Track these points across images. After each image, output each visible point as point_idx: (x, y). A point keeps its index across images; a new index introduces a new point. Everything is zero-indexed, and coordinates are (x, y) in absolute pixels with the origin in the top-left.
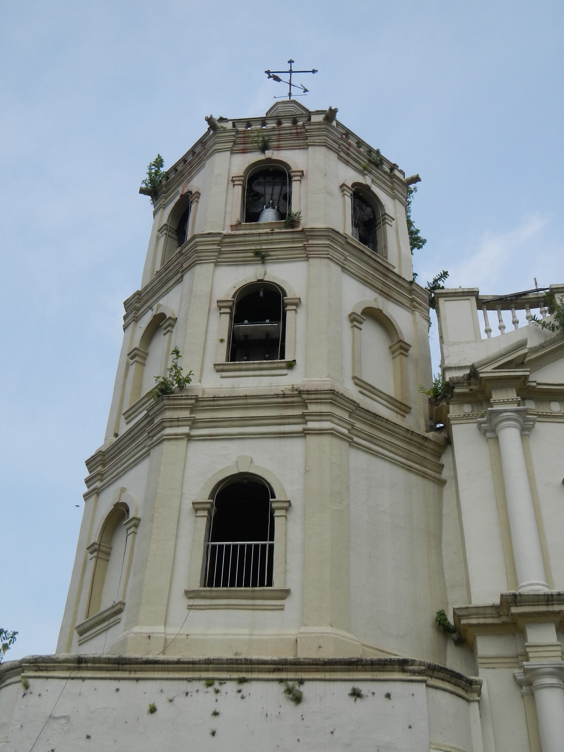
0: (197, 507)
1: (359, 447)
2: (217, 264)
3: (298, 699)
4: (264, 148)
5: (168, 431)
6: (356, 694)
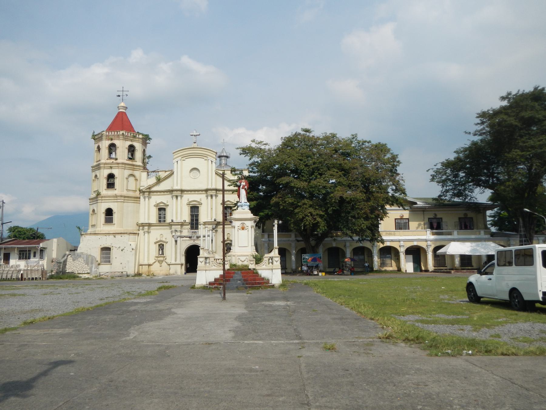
0: (103, 213)
1: (125, 202)
2: (104, 169)
3: (115, 237)
4: (112, 140)
5: (99, 201)
6: (121, 236)
